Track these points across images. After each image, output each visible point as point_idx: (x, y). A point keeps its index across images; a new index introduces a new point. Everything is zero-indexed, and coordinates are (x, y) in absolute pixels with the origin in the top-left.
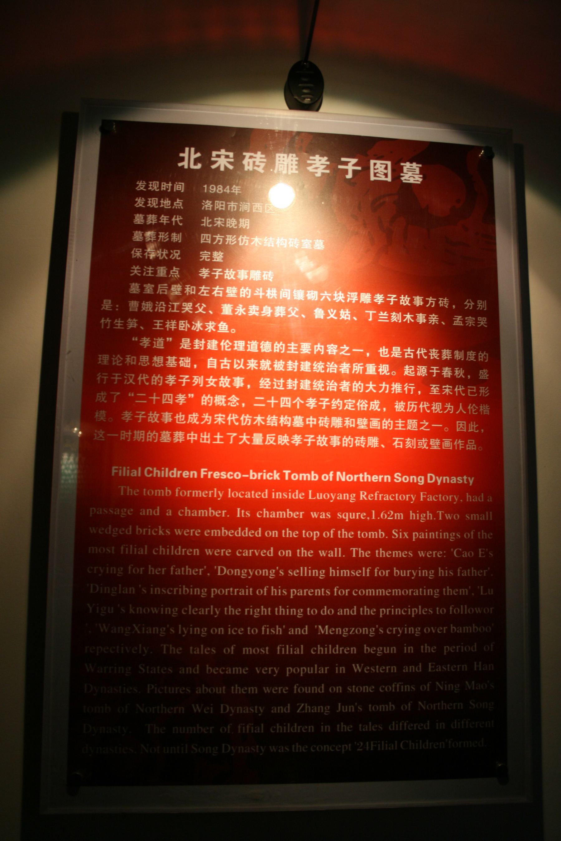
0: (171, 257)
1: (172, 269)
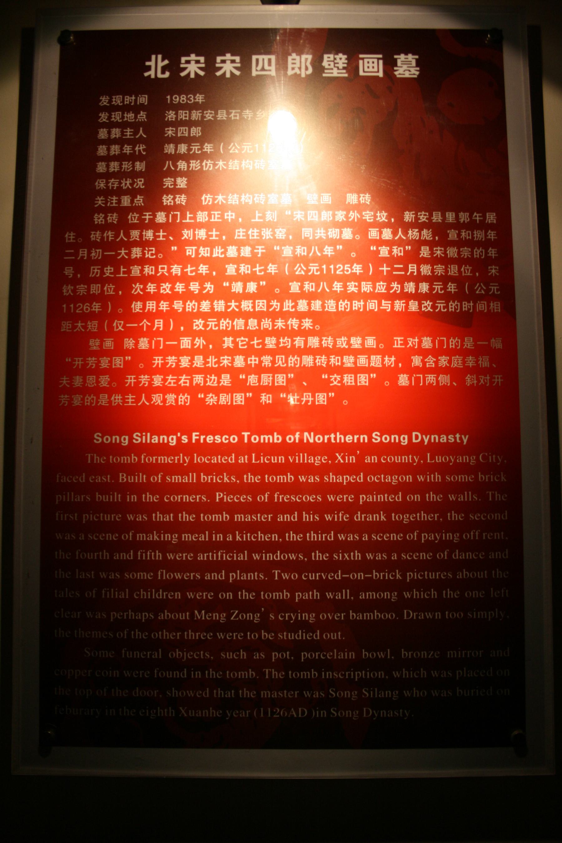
0: (135, 186)
1: (137, 198)
